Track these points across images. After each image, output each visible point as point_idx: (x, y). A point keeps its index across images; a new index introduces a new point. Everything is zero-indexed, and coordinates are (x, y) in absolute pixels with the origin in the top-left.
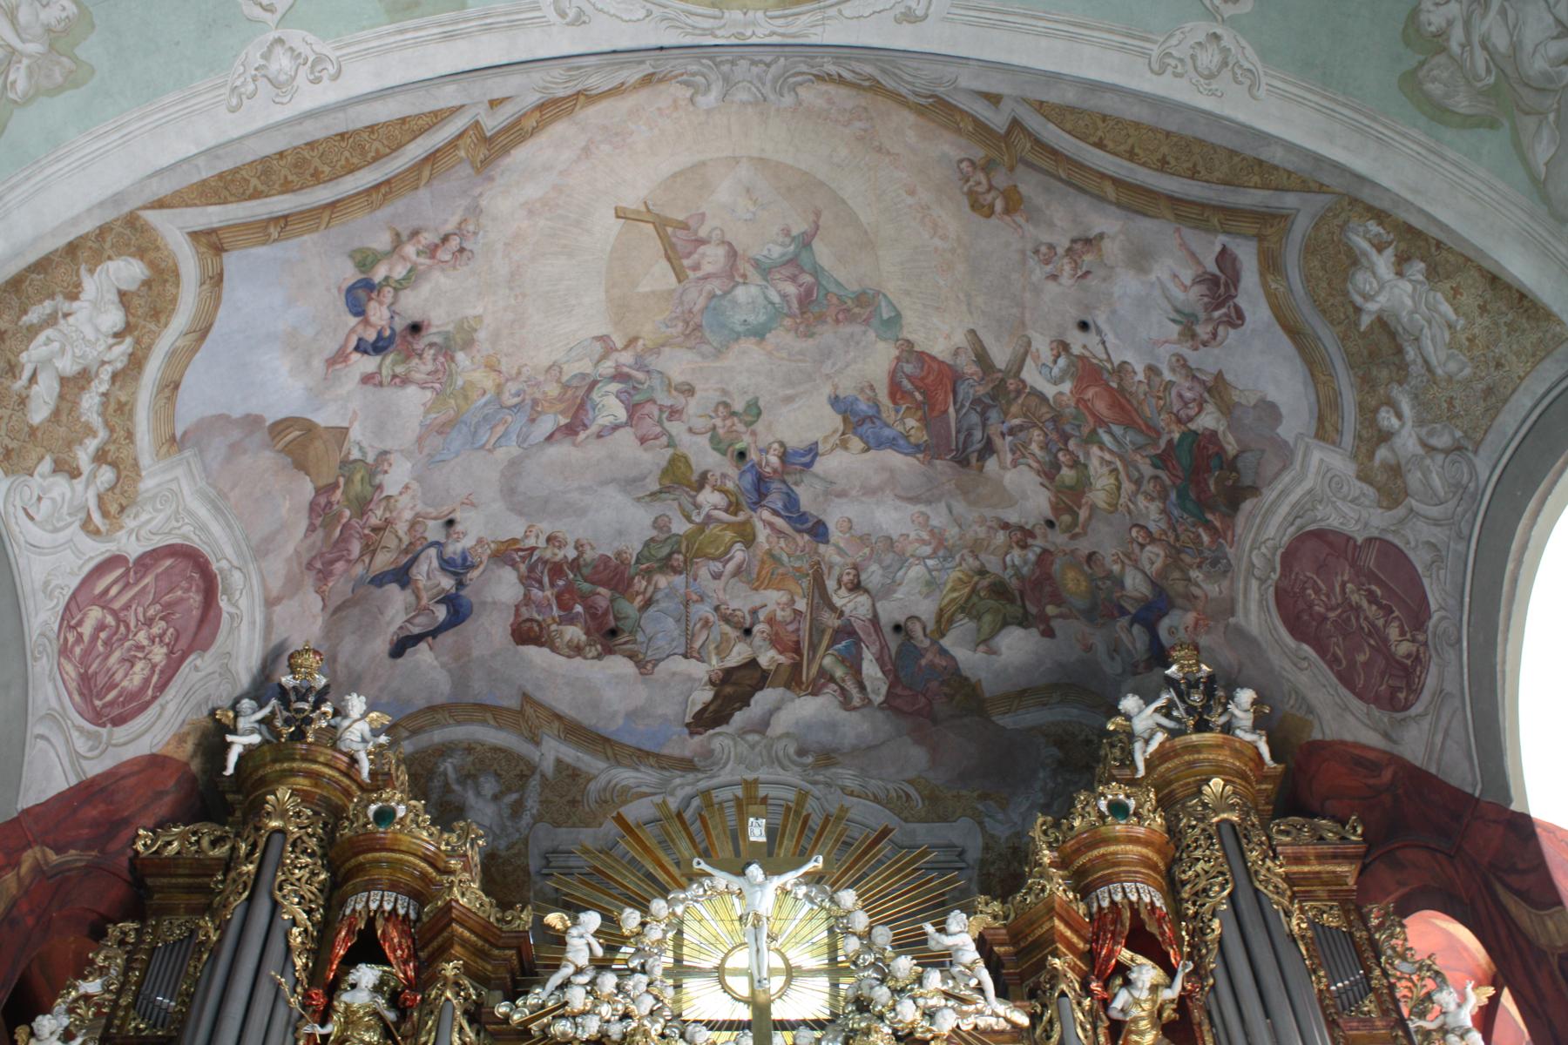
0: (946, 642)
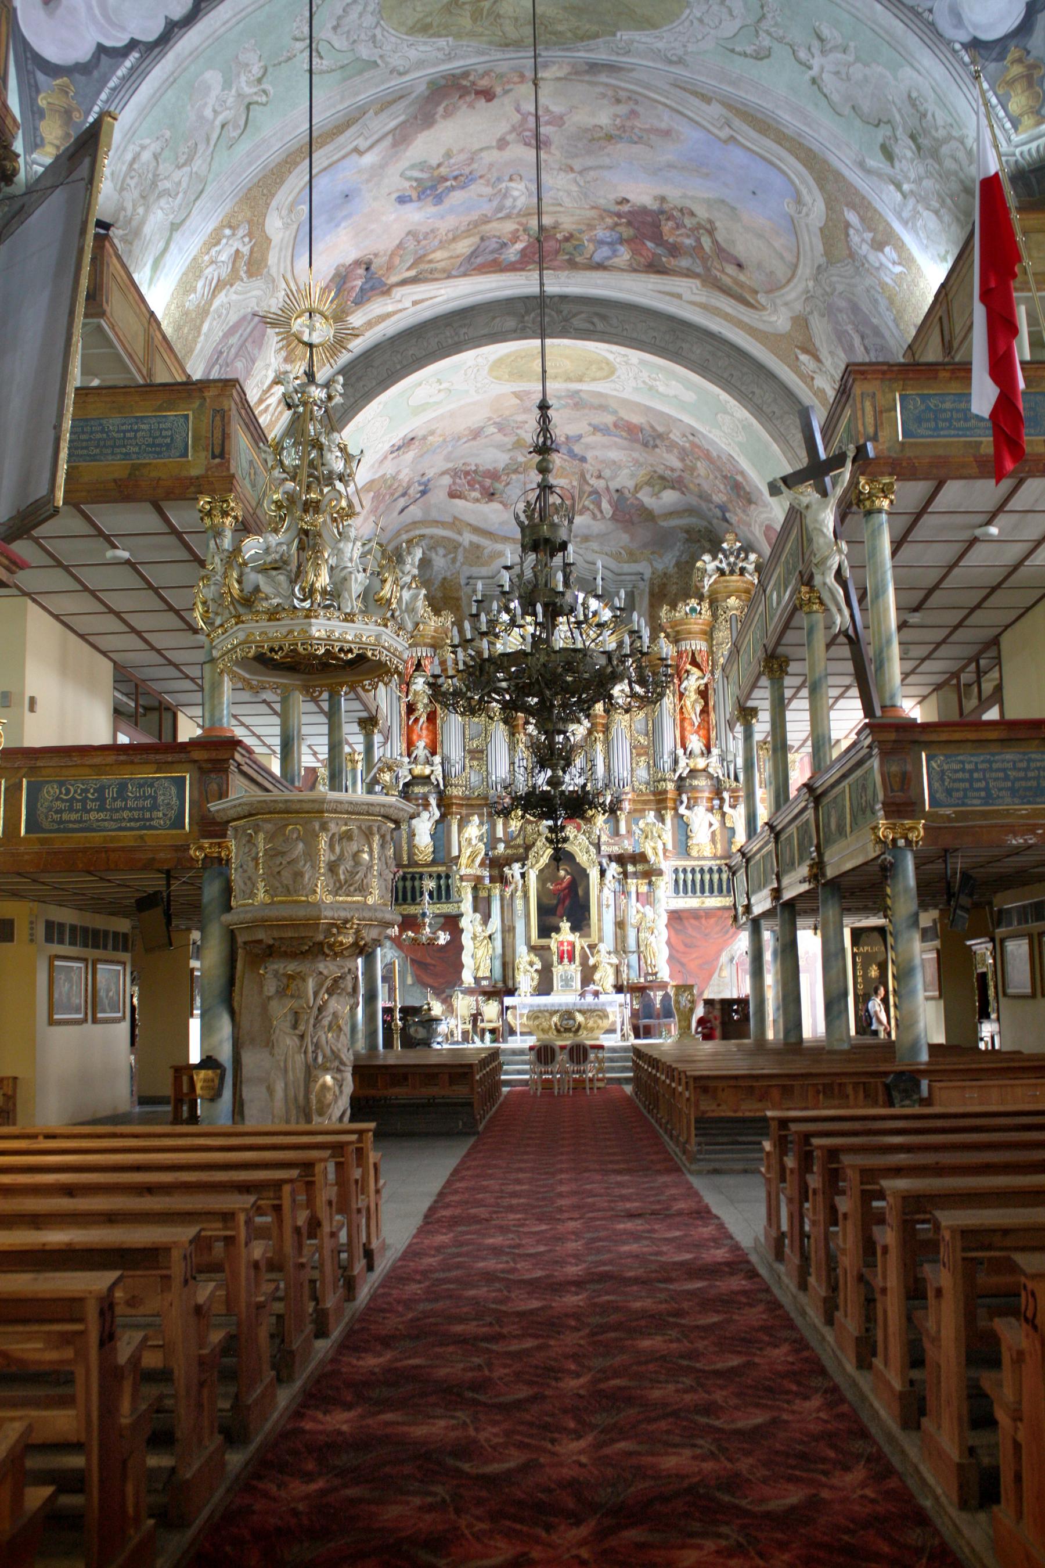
0: (639, 495)
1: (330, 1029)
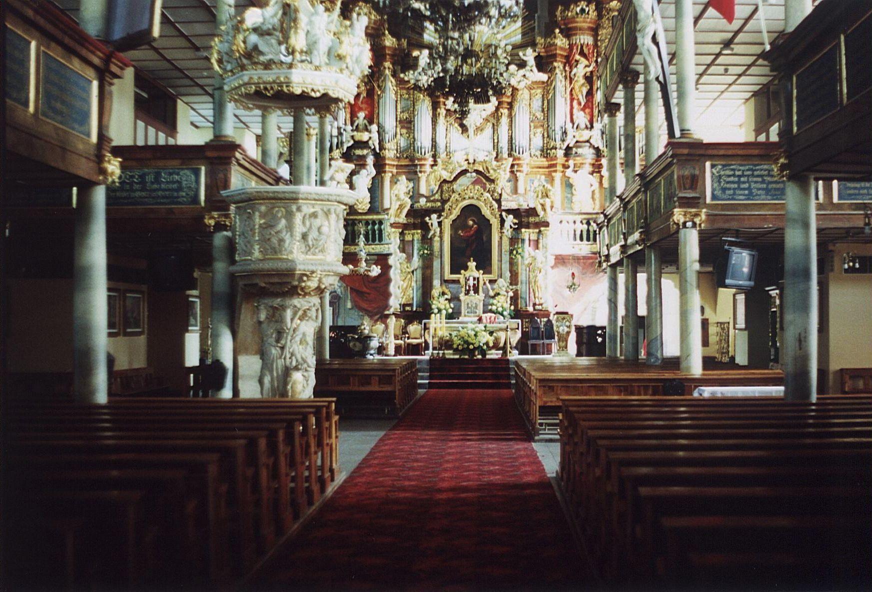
1: (301, 343)
